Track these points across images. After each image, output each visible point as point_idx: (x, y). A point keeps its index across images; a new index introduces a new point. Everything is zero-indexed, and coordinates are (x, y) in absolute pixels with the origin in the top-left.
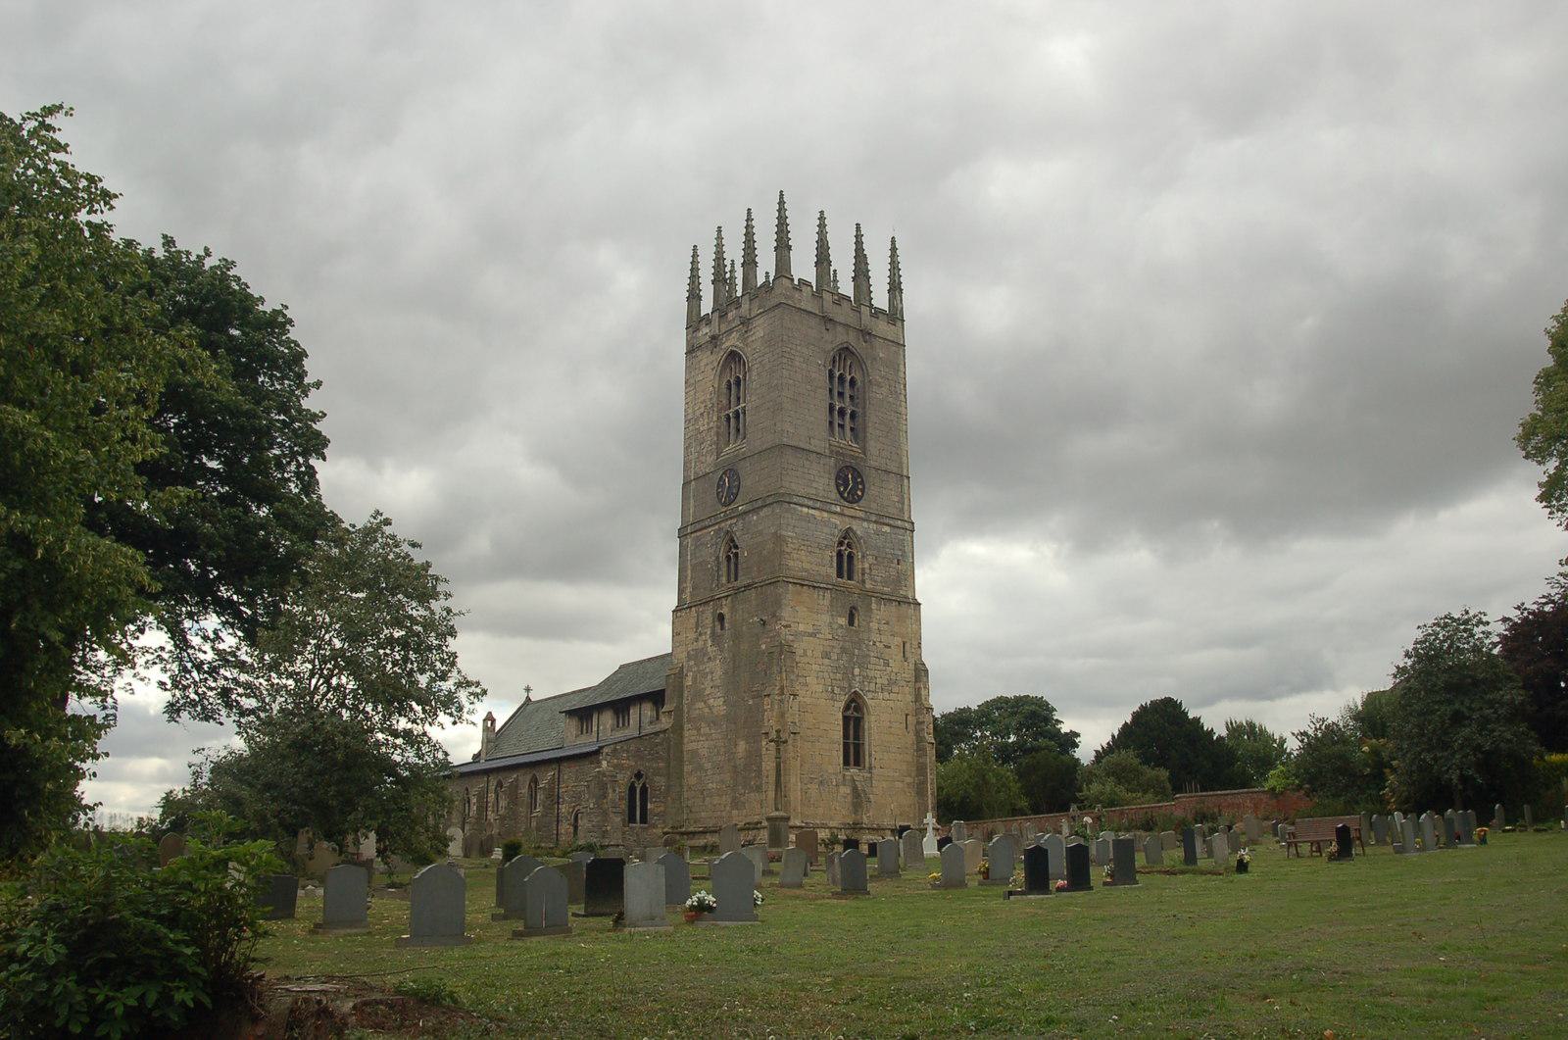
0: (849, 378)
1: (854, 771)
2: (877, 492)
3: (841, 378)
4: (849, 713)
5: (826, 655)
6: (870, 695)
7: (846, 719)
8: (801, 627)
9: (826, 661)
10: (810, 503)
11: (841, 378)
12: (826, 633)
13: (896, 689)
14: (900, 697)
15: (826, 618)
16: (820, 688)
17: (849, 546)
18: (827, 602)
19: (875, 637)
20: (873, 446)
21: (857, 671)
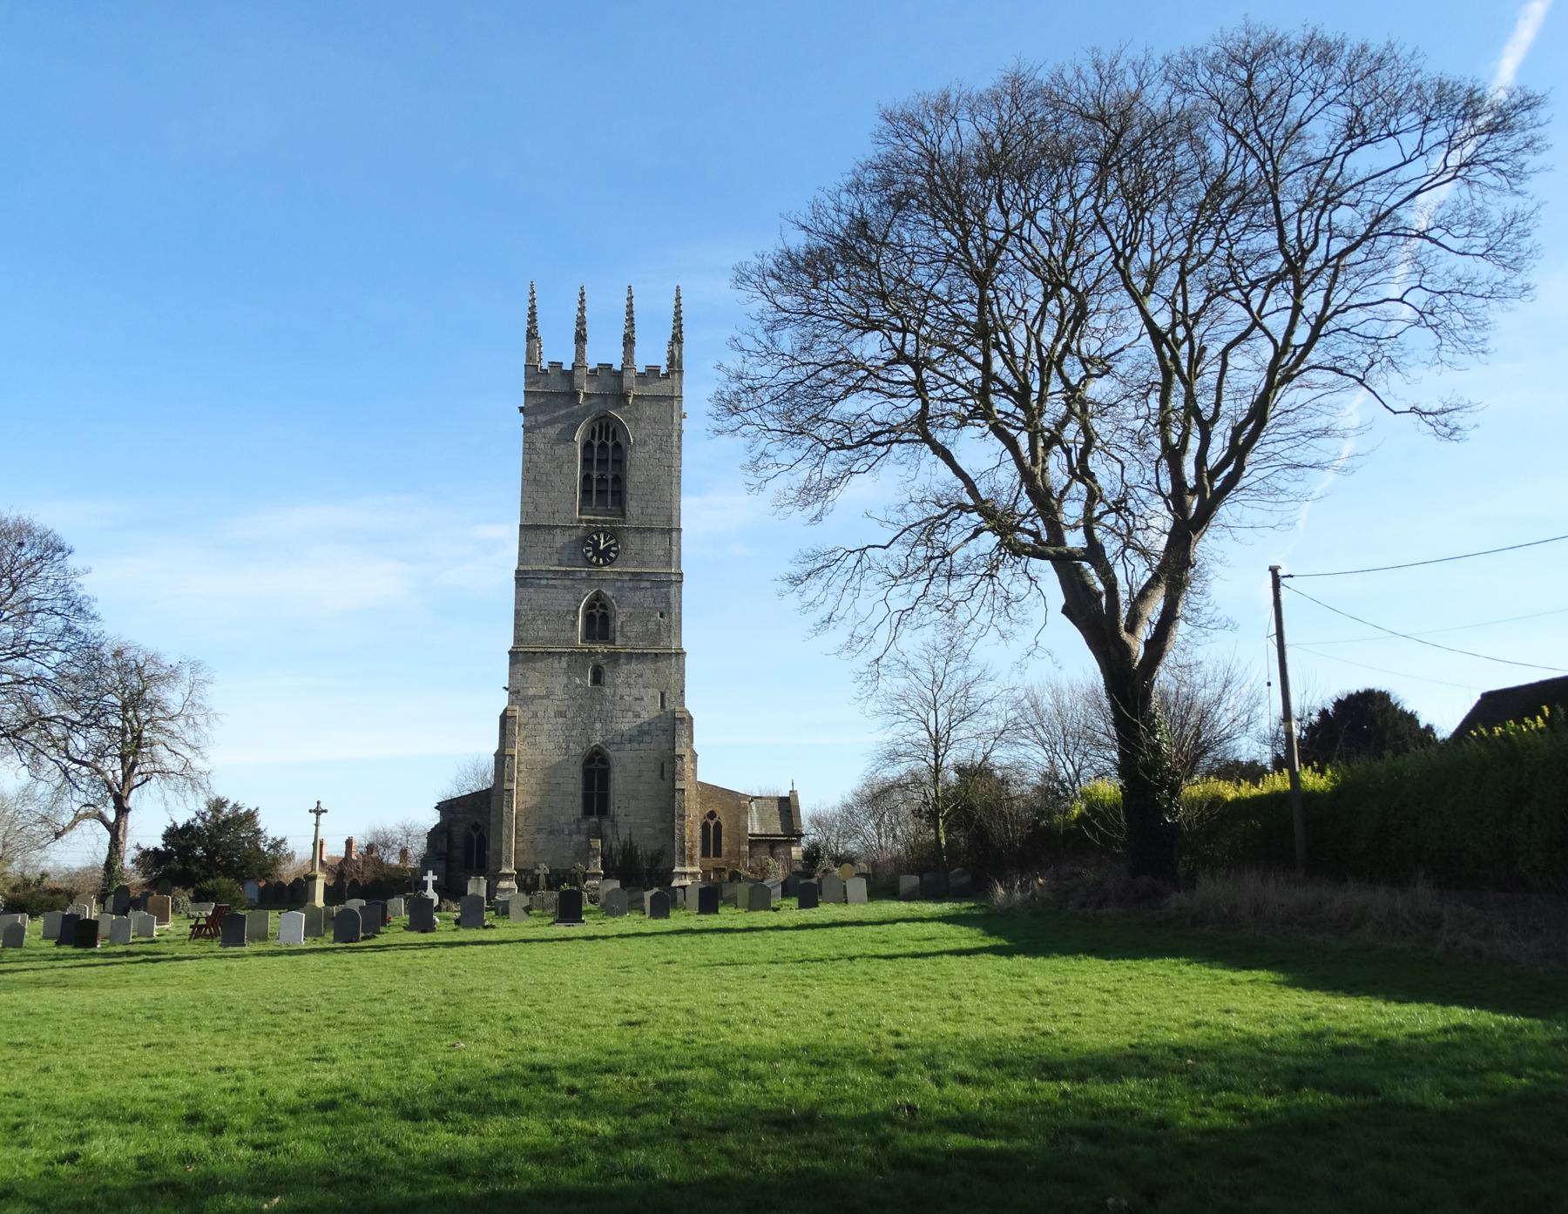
0: (610, 444)
1: (595, 819)
2: (636, 554)
3: (603, 446)
4: (592, 766)
5: (561, 714)
6: (614, 747)
7: (588, 774)
8: (531, 692)
9: (561, 720)
10: (550, 576)
11: (603, 446)
12: (559, 691)
13: (647, 738)
14: (652, 746)
15: (564, 680)
16: (551, 746)
17: (603, 606)
18: (564, 665)
19: (623, 690)
20: (633, 507)
21: (598, 726)
